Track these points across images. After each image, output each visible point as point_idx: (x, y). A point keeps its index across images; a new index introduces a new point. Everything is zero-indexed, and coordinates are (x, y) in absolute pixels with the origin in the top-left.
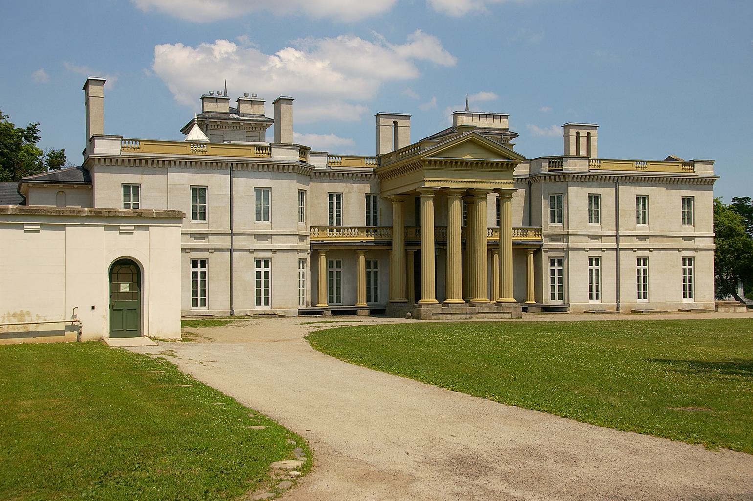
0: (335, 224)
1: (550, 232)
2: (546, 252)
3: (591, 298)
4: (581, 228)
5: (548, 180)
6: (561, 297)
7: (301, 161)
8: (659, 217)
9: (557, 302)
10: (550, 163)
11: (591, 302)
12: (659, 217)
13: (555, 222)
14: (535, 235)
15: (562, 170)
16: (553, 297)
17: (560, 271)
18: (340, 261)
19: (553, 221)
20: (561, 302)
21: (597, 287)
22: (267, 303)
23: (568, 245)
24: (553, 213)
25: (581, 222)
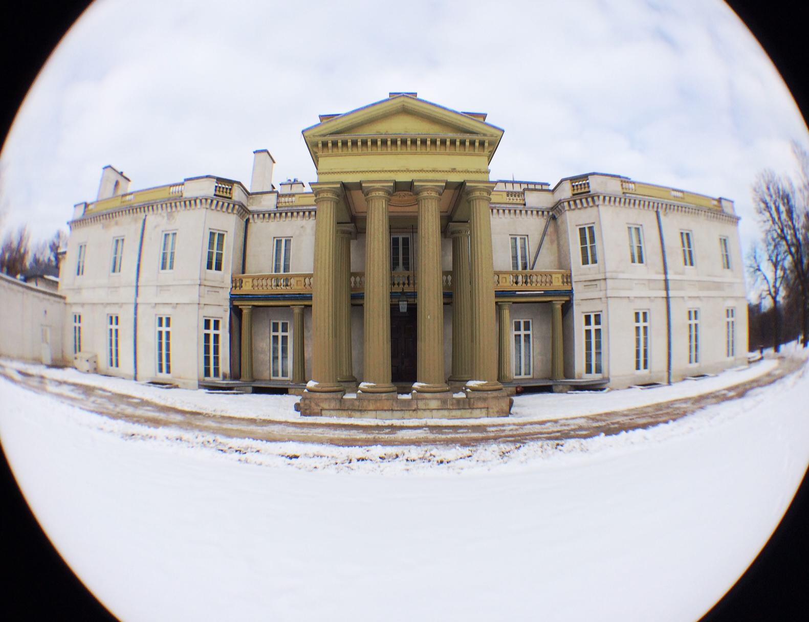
0: (282, 272)
1: (583, 278)
2: (579, 305)
3: (638, 368)
5: (573, 207)
6: (599, 370)
7: (215, 195)
9: (594, 377)
10: (573, 186)
13: (588, 264)
14: (563, 282)
16: (589, 370)
17: (598, 332)
18: (287, 323)
19: (585, 262)
22: (168, 372)
23: (606, 294)
24: (584, 250)
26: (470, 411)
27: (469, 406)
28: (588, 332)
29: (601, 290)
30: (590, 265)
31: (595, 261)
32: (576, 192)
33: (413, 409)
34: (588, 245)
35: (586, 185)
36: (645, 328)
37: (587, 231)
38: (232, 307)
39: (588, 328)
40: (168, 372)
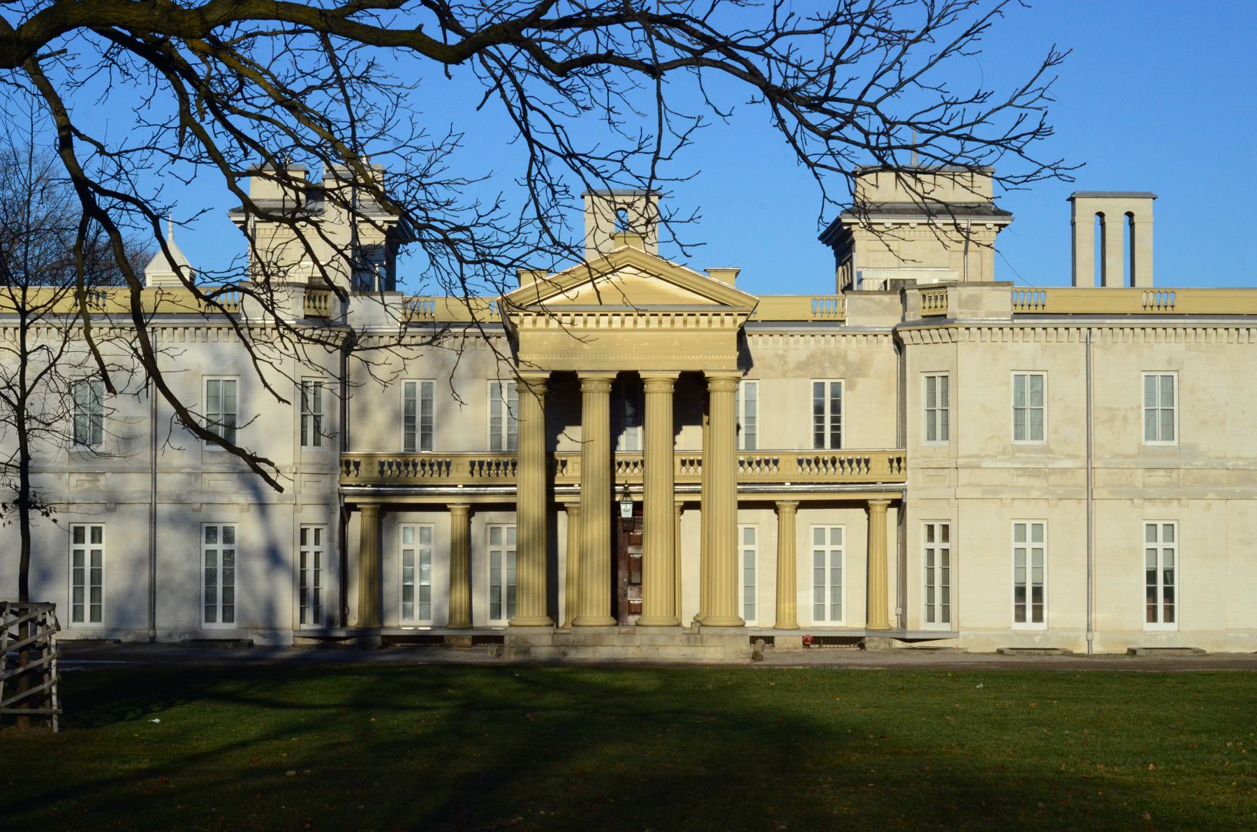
4: (992, 453)
6: (946, 618)
8: (1205, 423)
11: (1020, 626)
12: (1205, 423)
15: (945, 315)
16: (931, 618)
19: (932, 436)
20: (946, 627)
21: (1038, 592)
25: (992, 438)
26: (703, 649)
27: (701, 643)
28: (931, 552)
29: (950, 487)
30: (939, 443)
31: (946, 436)
32: (926, 313)
33: (637, 644)
34: (939, 405)
35: (944, 303)
36: (946, 552)
37: (939, 382)
38: (342, 505)
39: (931, 546)
40: (228, 617)
